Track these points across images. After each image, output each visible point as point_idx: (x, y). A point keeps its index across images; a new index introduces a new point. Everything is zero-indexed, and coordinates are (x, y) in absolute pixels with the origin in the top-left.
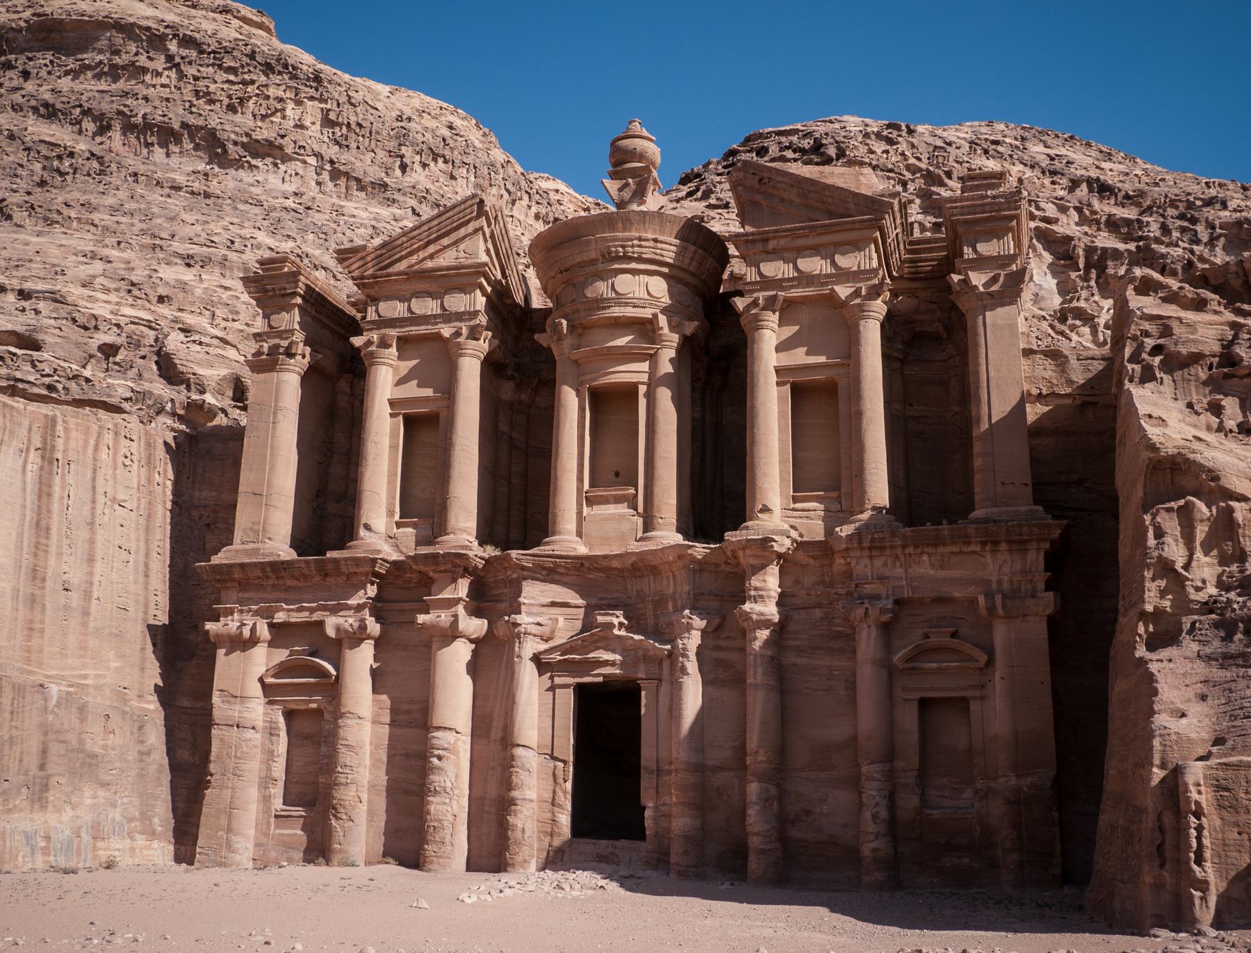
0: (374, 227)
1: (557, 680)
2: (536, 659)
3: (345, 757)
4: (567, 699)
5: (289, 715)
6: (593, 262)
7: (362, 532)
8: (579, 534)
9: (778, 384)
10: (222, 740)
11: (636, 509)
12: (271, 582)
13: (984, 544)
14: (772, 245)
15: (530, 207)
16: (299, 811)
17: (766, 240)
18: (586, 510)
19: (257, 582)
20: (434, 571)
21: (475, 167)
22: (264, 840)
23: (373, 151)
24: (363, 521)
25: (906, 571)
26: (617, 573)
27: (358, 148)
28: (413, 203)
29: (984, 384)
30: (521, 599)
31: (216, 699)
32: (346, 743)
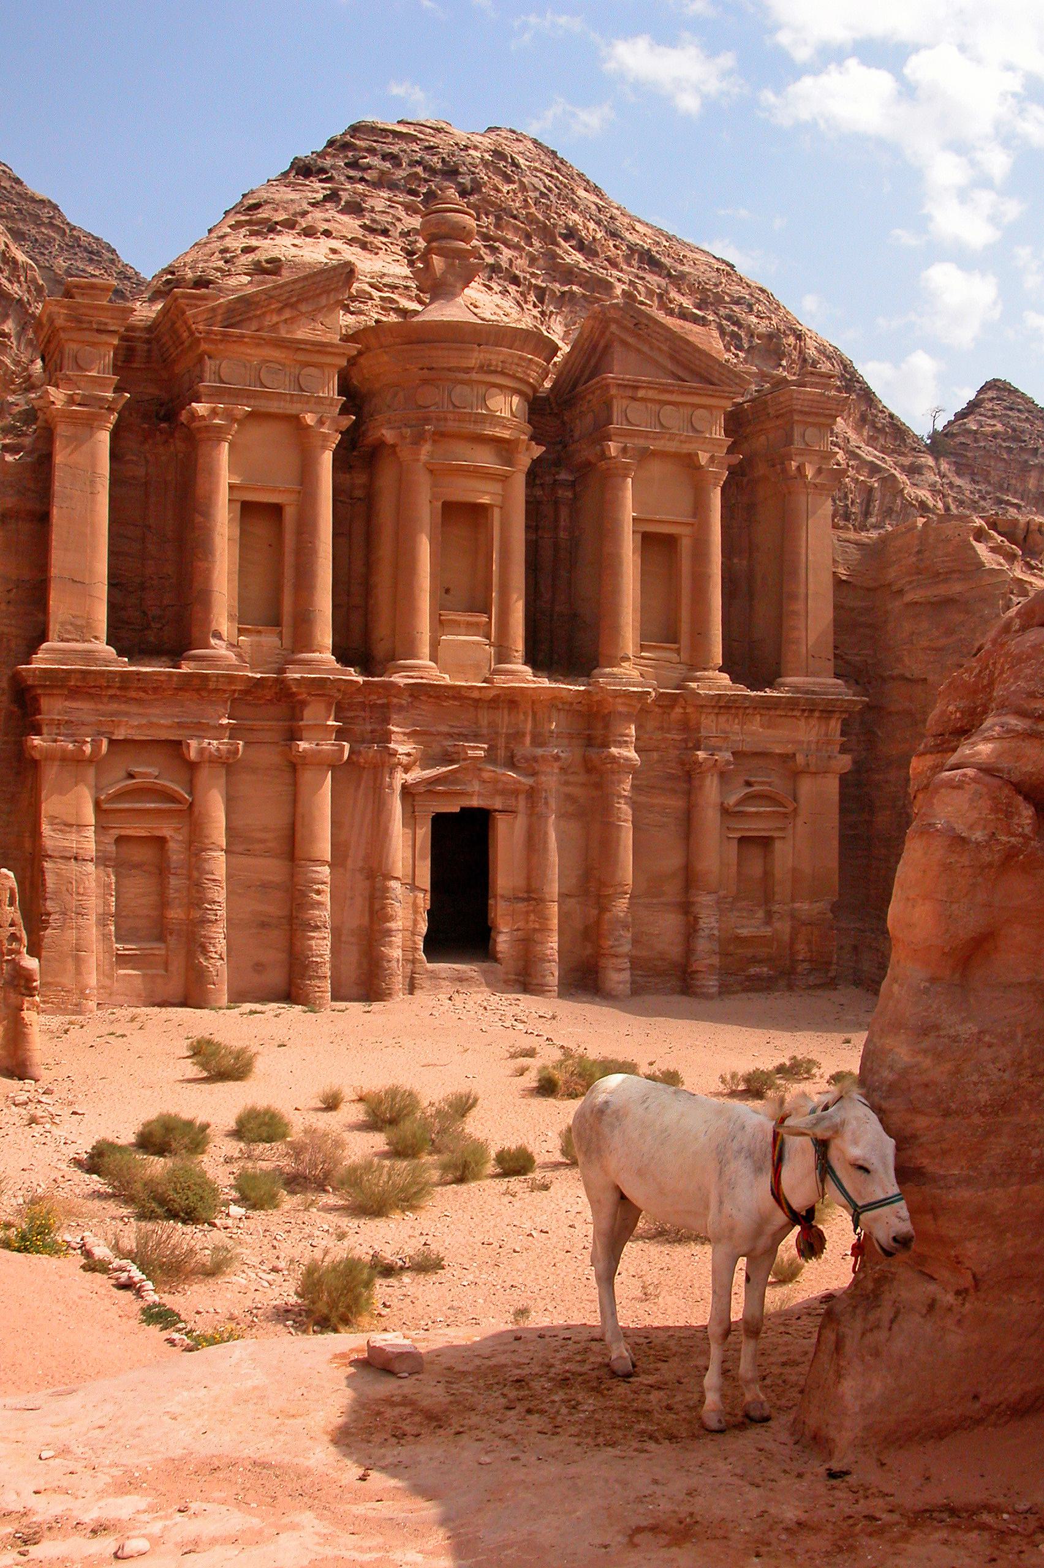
6: (468, 370)
7: (213, 641)
8: (434, 658)
10: (58, 874)
11: (488, 637)
12: (111, 692)
13: (804, 711)
14: (641, 393)
17: (637, 388)
19: (93, 691)
20: (309, 694)
22: (107, 982)
25: (742, 728)
26: (470, 702)
29: (803, 565)
32: (213, 877)
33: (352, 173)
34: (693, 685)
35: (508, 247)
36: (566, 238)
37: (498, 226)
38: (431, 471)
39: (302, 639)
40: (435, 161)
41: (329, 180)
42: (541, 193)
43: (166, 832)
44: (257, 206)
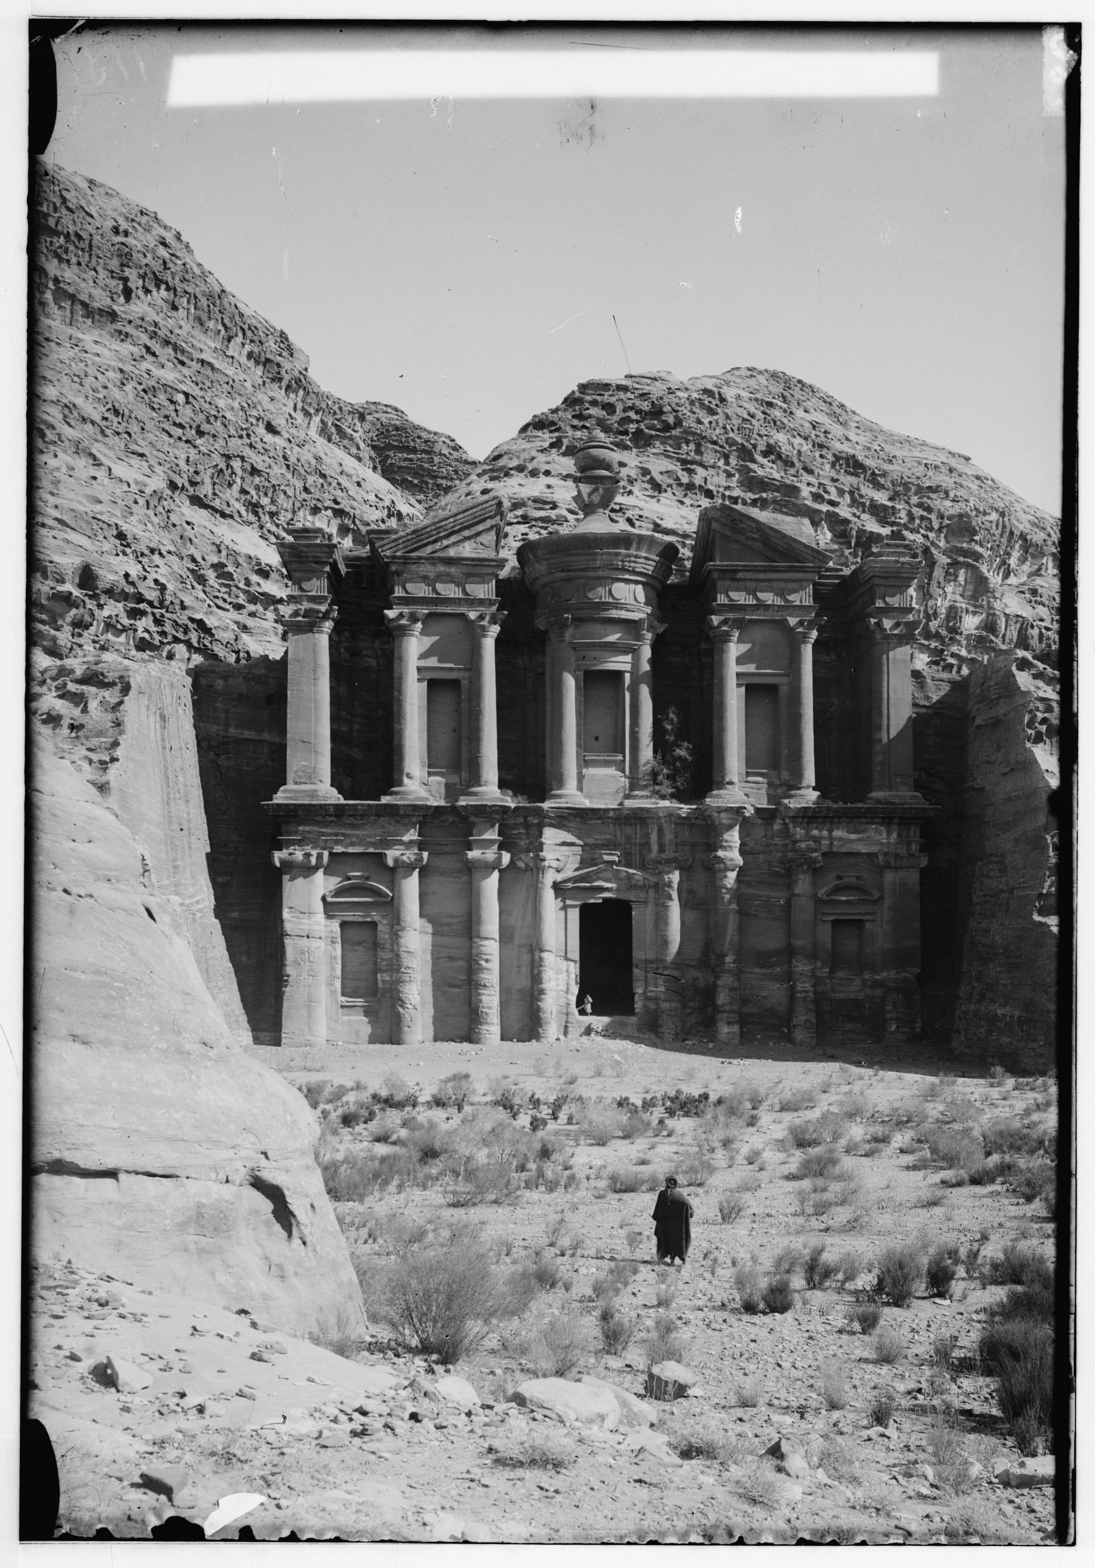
0: (121, 371)
1: (568, 902)
2: (556, 886)
3: (407, 961)
4: (574, 915)
5: (344, 925)
6: (595, 569)
7: (406, 780)
8: (580, 788)
9: (738, 685)
11: (623, 771)
14: (740, 575)
15: (243, 344)
16: (360, 1001)
17: (736, 571)
18: (584, 771)
21: (196, 297)
23: (95, 270)
24: (406, 770)
27: (79, 264)
28: (145, 339)
29: (885, 701)
30: (543, 840)
31: (286, 914)
33: (576, 422)
34: (786, 801)
35: (705, 467)
36: (765, 454)
37: (698, 452)
38: (574, 648)
39: (475, 777)
40: (645, 406)
41: (558, 430)
42: (744, 419)
43: (377, 918)
44: (499, 457)
